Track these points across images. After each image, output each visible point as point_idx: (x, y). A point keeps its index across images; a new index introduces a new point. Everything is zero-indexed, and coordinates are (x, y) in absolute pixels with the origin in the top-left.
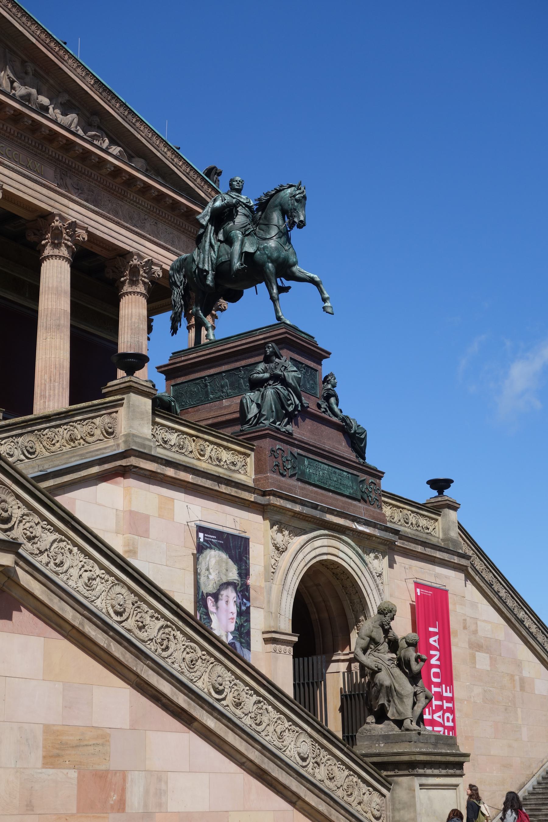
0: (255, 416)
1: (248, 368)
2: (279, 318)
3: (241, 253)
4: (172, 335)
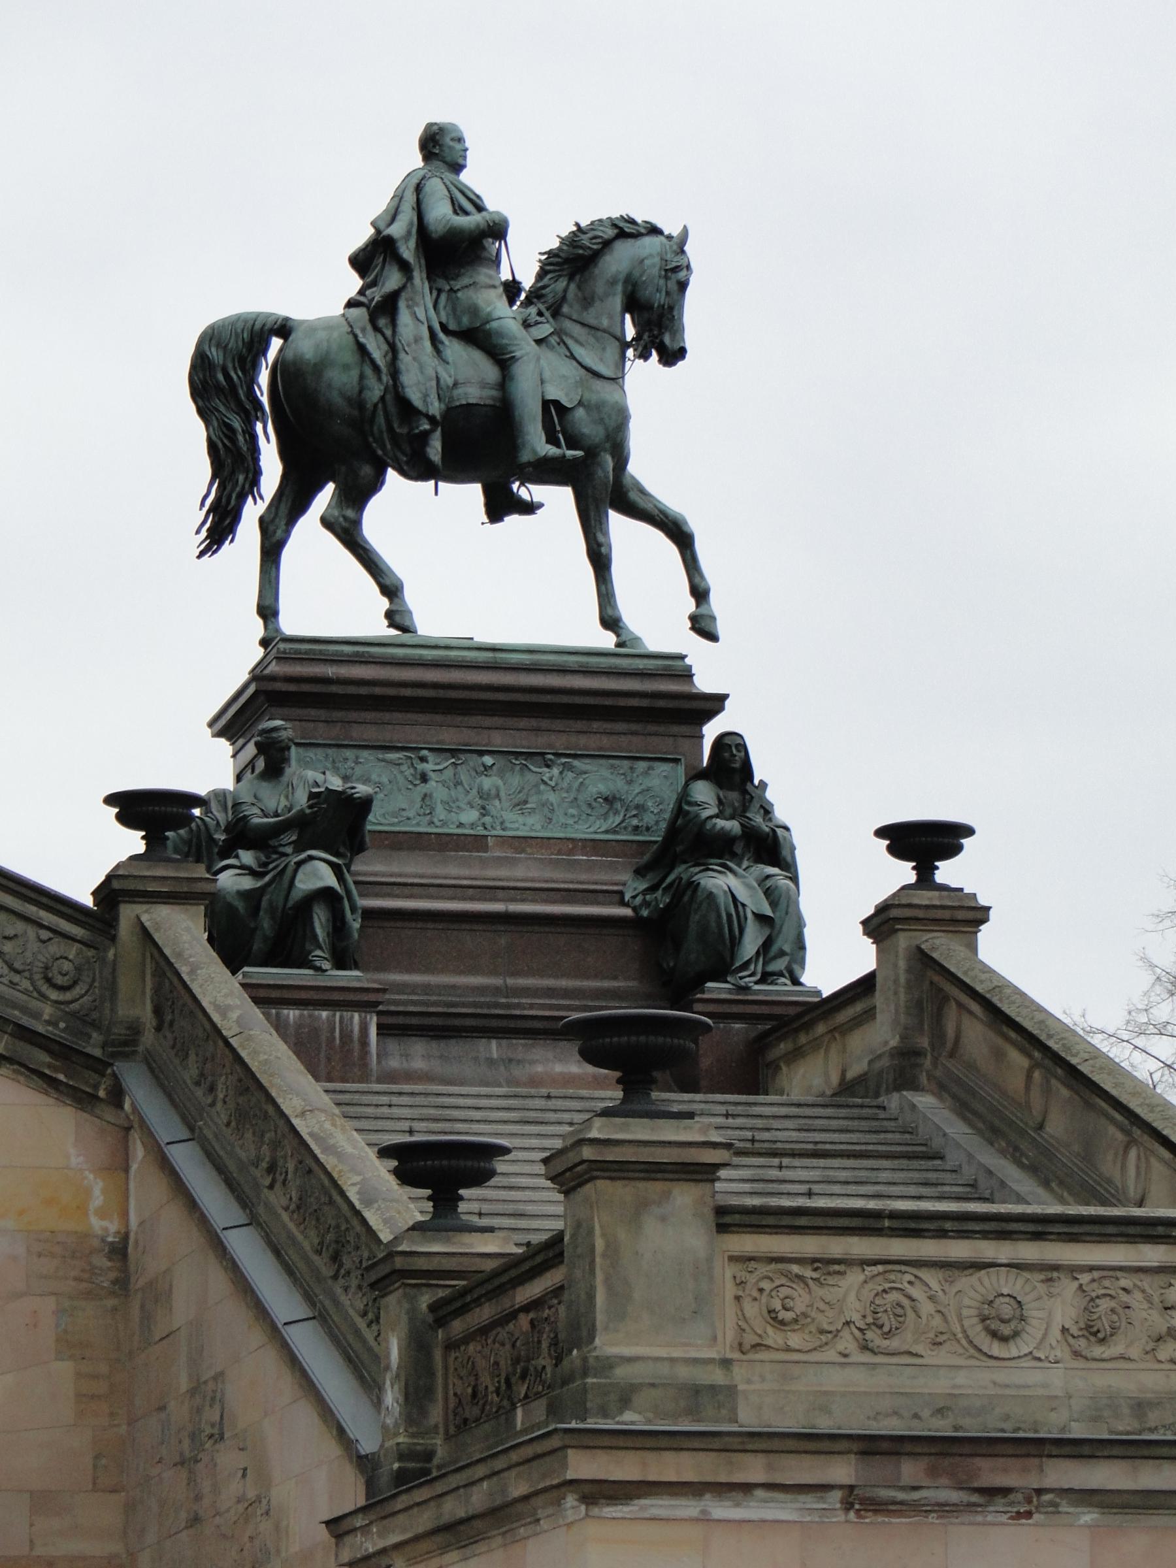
0: (758, 953)
1: (576, 763)
2: (611, 622)
3: (546, 404)
4: (202, 554)
